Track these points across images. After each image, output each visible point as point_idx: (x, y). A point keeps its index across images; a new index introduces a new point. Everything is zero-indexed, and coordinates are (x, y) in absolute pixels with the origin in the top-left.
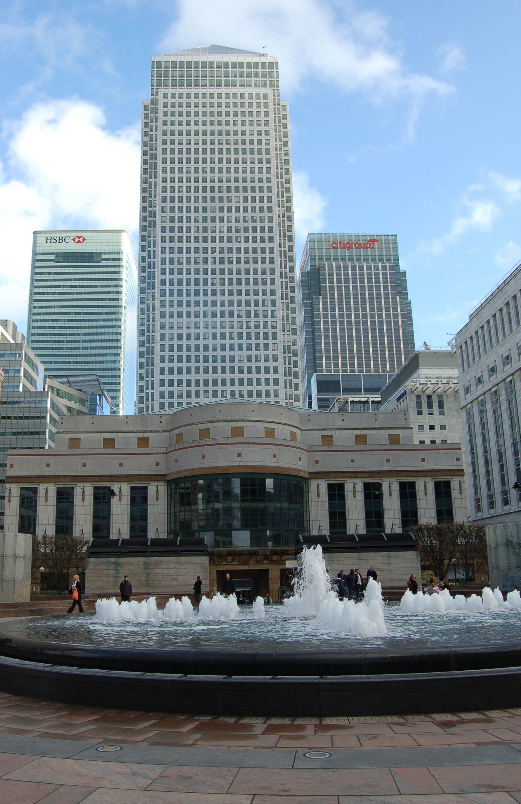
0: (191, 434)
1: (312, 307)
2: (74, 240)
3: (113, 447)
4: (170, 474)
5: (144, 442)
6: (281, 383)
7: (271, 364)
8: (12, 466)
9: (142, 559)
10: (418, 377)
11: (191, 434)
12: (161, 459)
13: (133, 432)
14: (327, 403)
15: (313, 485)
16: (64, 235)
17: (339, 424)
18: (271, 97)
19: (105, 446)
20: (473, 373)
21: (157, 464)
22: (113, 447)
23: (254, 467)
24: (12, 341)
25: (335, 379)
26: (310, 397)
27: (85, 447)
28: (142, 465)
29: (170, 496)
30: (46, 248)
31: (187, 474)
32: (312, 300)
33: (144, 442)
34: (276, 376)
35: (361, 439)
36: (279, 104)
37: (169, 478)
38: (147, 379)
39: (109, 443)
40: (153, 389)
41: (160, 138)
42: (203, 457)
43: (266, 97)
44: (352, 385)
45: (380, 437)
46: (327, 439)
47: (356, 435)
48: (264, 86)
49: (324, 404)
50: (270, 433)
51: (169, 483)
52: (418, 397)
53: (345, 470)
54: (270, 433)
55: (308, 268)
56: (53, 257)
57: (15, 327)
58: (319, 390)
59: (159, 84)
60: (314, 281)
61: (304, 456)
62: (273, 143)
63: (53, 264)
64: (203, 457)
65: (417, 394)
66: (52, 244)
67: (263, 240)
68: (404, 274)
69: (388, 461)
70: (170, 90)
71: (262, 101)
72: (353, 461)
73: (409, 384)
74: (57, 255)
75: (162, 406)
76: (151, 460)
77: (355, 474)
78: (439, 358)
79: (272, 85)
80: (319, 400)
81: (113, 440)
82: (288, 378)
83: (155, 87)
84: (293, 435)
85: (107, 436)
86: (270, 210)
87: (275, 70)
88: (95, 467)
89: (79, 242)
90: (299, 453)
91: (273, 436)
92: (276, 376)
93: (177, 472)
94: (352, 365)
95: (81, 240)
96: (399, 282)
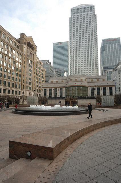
0: (69, 80)
5: (62, 81)
6: (95, 68)
7: (93, 65)
11: (69, 80)
12: (64, 84)
15: (89, 88)
18: (93, 13)
19: (57, 82)
27: (54, 82)
28: (62, 85)
33: (62, 81)
43: (92, 13)
44: (110, 67)
46: (92, 80)
50: (82, 80)
51: (66, 88)
54: (82, 80)
57: (49, 61)
58: (104, 69)
60: (103, 48)
61: (87, 83)
67: (91, 42)
73: (117, 68)
74: (57, 47)
75: (74, 73)
77: (95, 86)
84: (86, 80)
86: (93, 36)
90: (86, 83)
91: (82, 80)
94: (110, 64)
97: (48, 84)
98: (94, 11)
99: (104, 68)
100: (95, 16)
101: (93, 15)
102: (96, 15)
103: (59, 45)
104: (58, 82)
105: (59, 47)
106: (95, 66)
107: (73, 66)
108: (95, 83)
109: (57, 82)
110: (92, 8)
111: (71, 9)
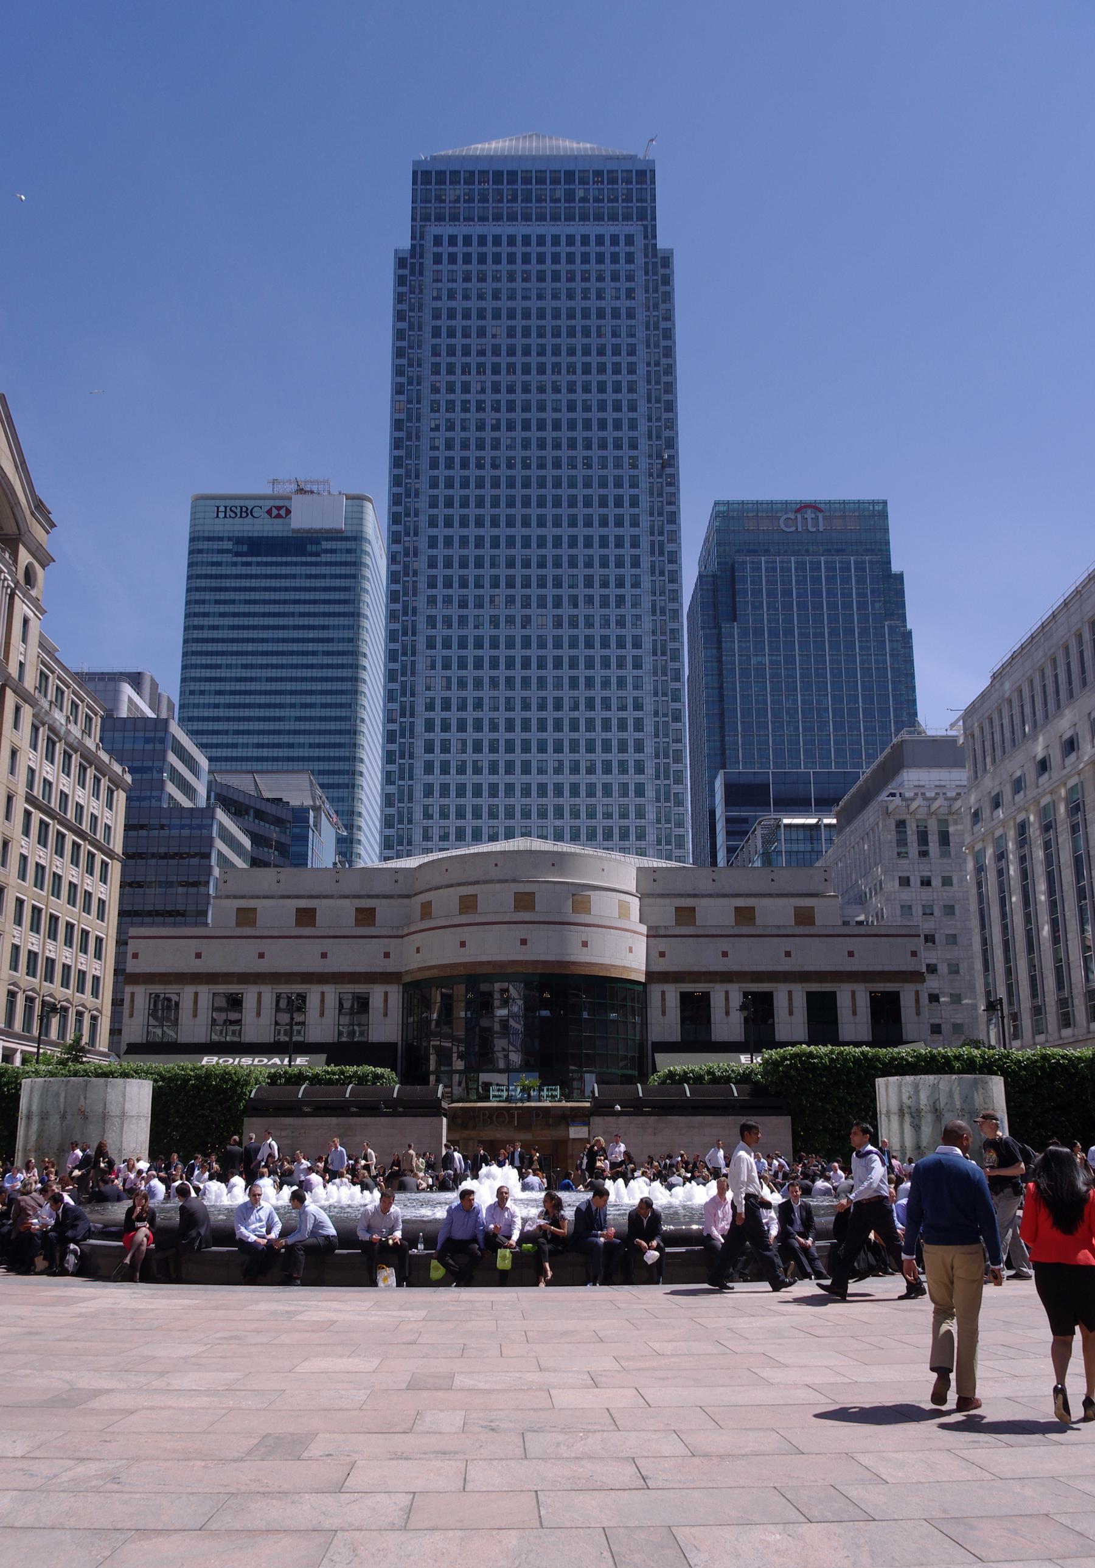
1: (719, 642)
2: (269, 512)
3: (314, 925)
4: (408, 972)
5: (366, 916)
6: (650, 793)
8: (135, 956)
9: (334, 1120)
10: (901, 785)
13: (347, 897)
14: (744, 827)
16: (250, 504)
17: (706, 886)
20: (989, 784)
21: (387, 955)
22: (314, 925)
23: (545, 963)
24: (151, 714)
25: (758, 781)
26: (712, 813)
29: (408, 1009)
30: (217, 528)
31: (435, 973)
32: (720, 628)
34: (640, 778)
35: (745, 915)
36: (655, 255)
37: (407, 979)
38: (401, 783)
39: (306, 917)
40: (410, 800)
41: (429, 323)
42: (463, 944)
43: (630, 240)
45: (776, 912)
47: (736, 908)
48: (627, 217)
49: (738, 830)
52: (901, 824)
53: (712, 969)
55: (714, 567)
56: (228, 545)
57: (154, 685)
58: (729, 802)
59: (426, 218)
62: (641, 334)
63: (229, 558)
64: (463, 944)
65: (898, 817)
66: (228, 521)
68: (900, 577)
69: (788, 954)
70: (446, 230)
71: (622, 249)
72: (725, 954)
74: (239, 541)
76: (376, 947)
78: (941, 752)
79: (642, 216)
80: (729, 821)
81: (313, 911)
82: (662, 782)
83: (418, 223)
85: (303, 903)
87: (648, 186)
88: (283, 957)
89: (279, 516)
92: (640, 778)
93: (421, 969)
95: (283, 512)
96: (890, 590)
97: (193, 945)
98: (647, 215)
99: (736, 794)
100: (661, 265)
101: (640, 259)
102: (667, 261)
103: (263, 526)
104: (313, 924)
105: (256, 546)
106: (650, 770)
107: (421, 757)
108: (725, 945)
109: (306, 917)
110: (628, 189)
111: (416, 163)
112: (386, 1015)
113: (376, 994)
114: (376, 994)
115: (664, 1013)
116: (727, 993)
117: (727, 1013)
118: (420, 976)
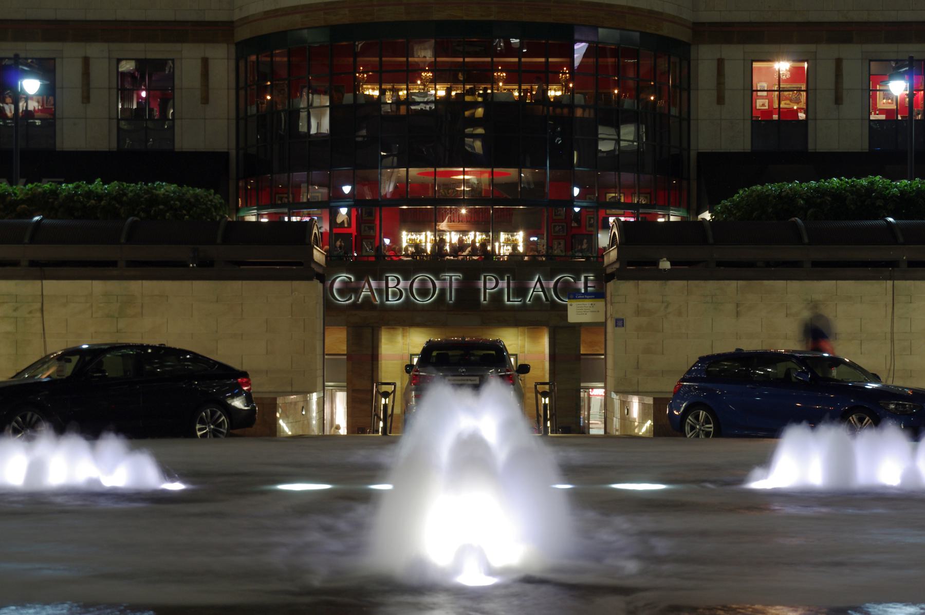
4: (246, 21)
9: (98, 286)
37: (243, 34)
51: (244, 48)
53: (813, 17)
112: (205, 100)
113: (187, 60)
114: (187, 60)
115: (720, 100)
116: (839, 62)
117: (838, 100)
118: (268, 27)
